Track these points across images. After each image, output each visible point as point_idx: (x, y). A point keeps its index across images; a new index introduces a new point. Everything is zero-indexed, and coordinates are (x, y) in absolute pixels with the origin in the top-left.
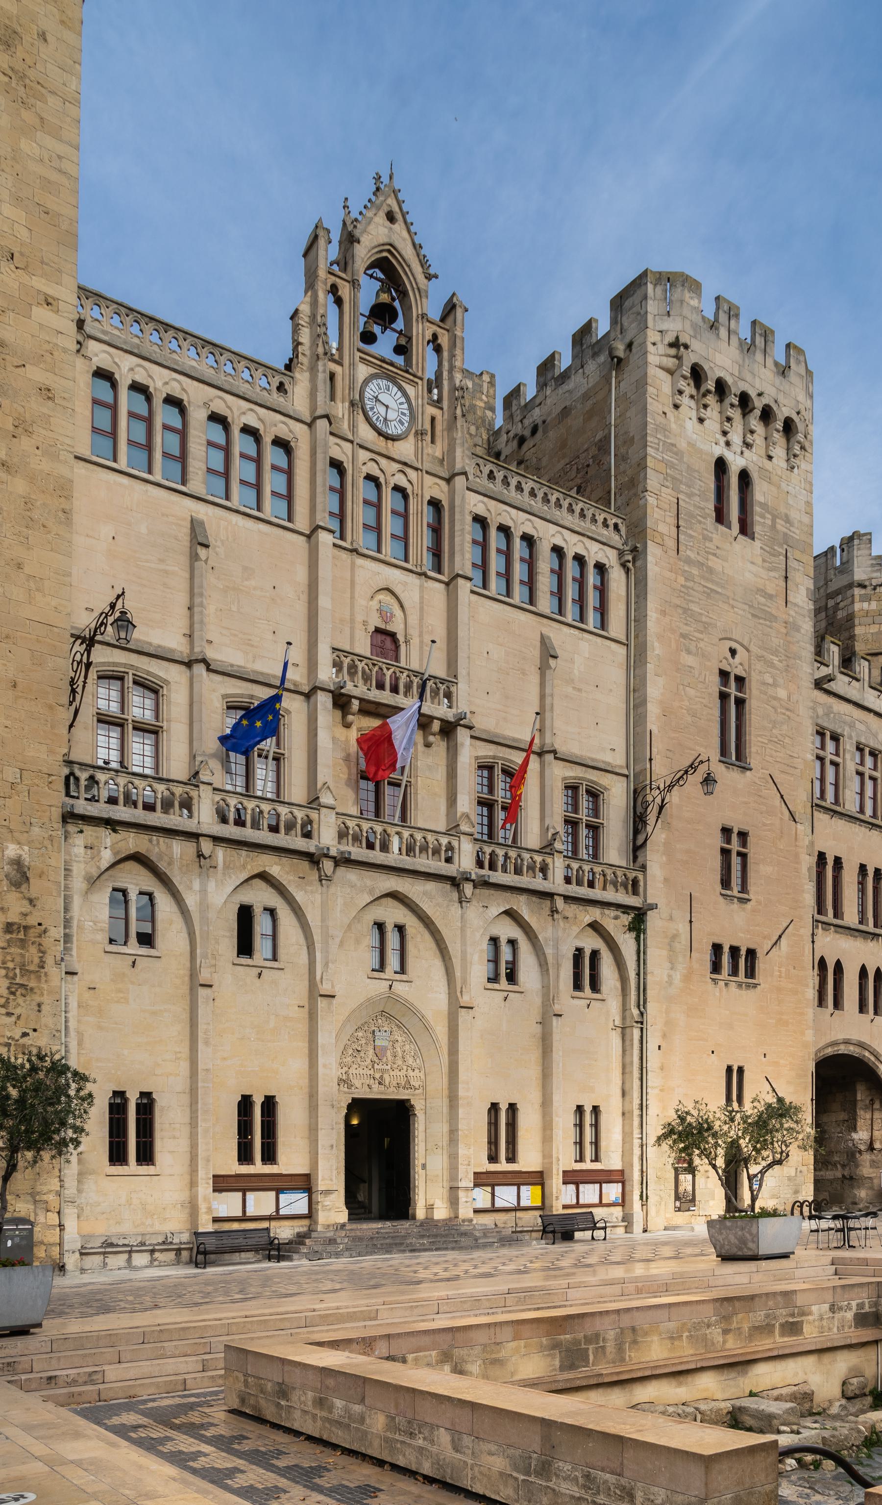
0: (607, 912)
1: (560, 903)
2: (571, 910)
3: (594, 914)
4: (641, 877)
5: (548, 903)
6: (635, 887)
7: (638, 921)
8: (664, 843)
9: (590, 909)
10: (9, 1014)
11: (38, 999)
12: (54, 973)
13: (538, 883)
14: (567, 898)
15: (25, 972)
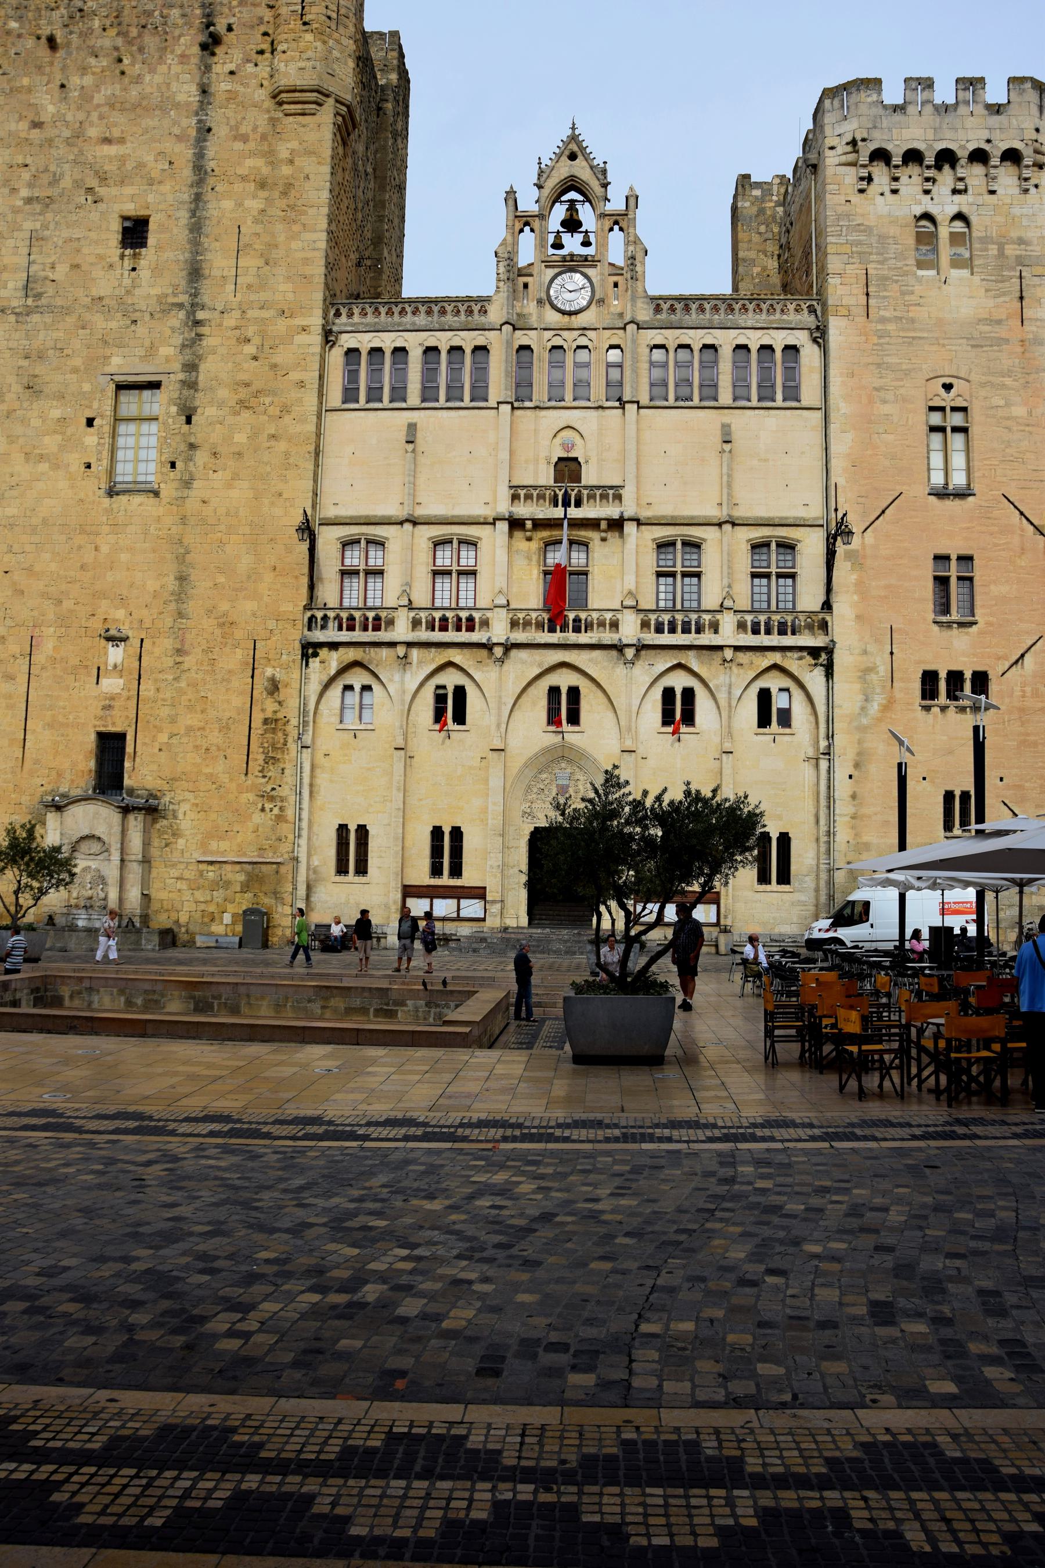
0: (789, 654)
1: (728, 654)
2: (742, 657)
3: (776, 658)
4: (828, 618)
5: (720, 653)
6: (824, 626)
7: (823, 657)
8: (856, 585)
9: (769, 654)
10: (264, 777)
11: (282, 766)
12: (292, 746)
13: (707, 638)
14: (737, 648)
15: (275, 748)
